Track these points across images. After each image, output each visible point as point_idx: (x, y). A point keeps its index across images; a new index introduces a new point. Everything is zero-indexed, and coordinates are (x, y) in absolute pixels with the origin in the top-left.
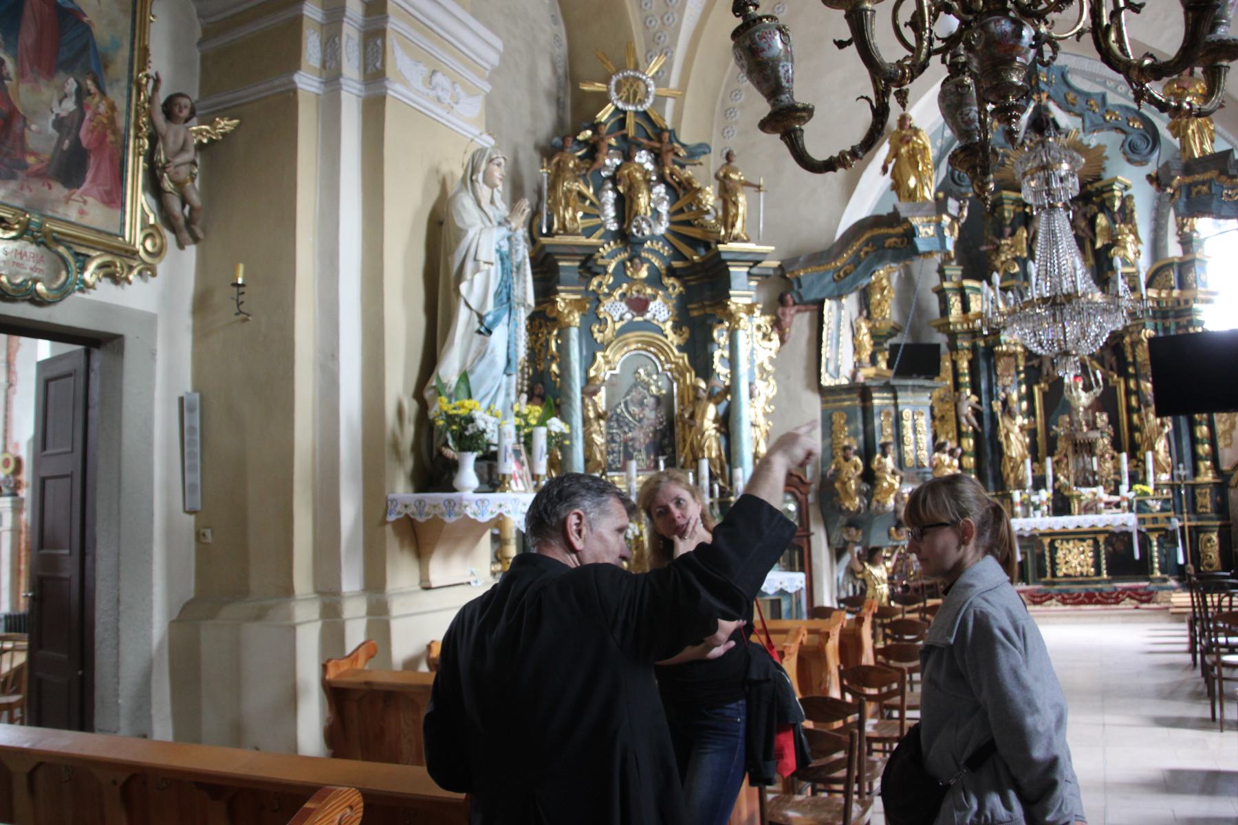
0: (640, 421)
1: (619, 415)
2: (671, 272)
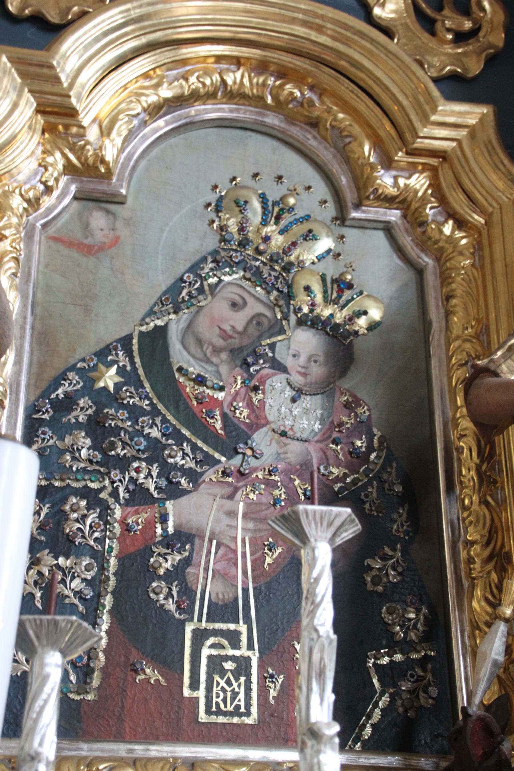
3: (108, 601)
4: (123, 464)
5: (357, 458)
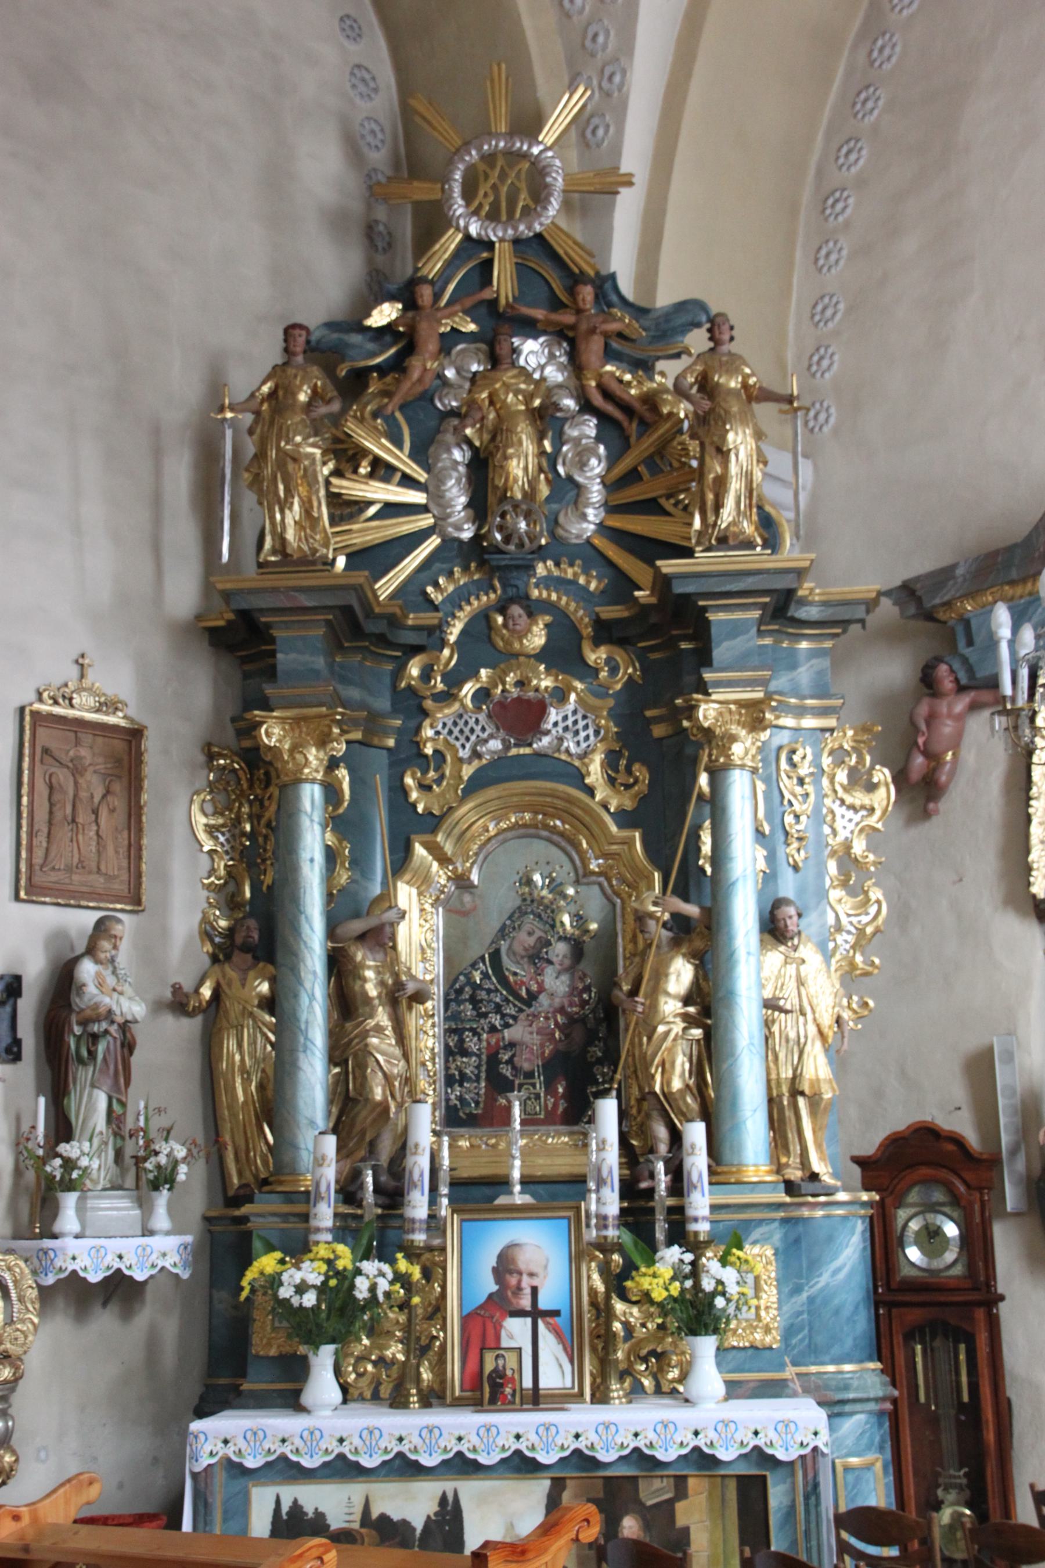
0: (532, 997)
1: (476, 987)
2: (605, 632)
3: (483, 1075)
4: (485, 1015)
5: (584, 1003)
